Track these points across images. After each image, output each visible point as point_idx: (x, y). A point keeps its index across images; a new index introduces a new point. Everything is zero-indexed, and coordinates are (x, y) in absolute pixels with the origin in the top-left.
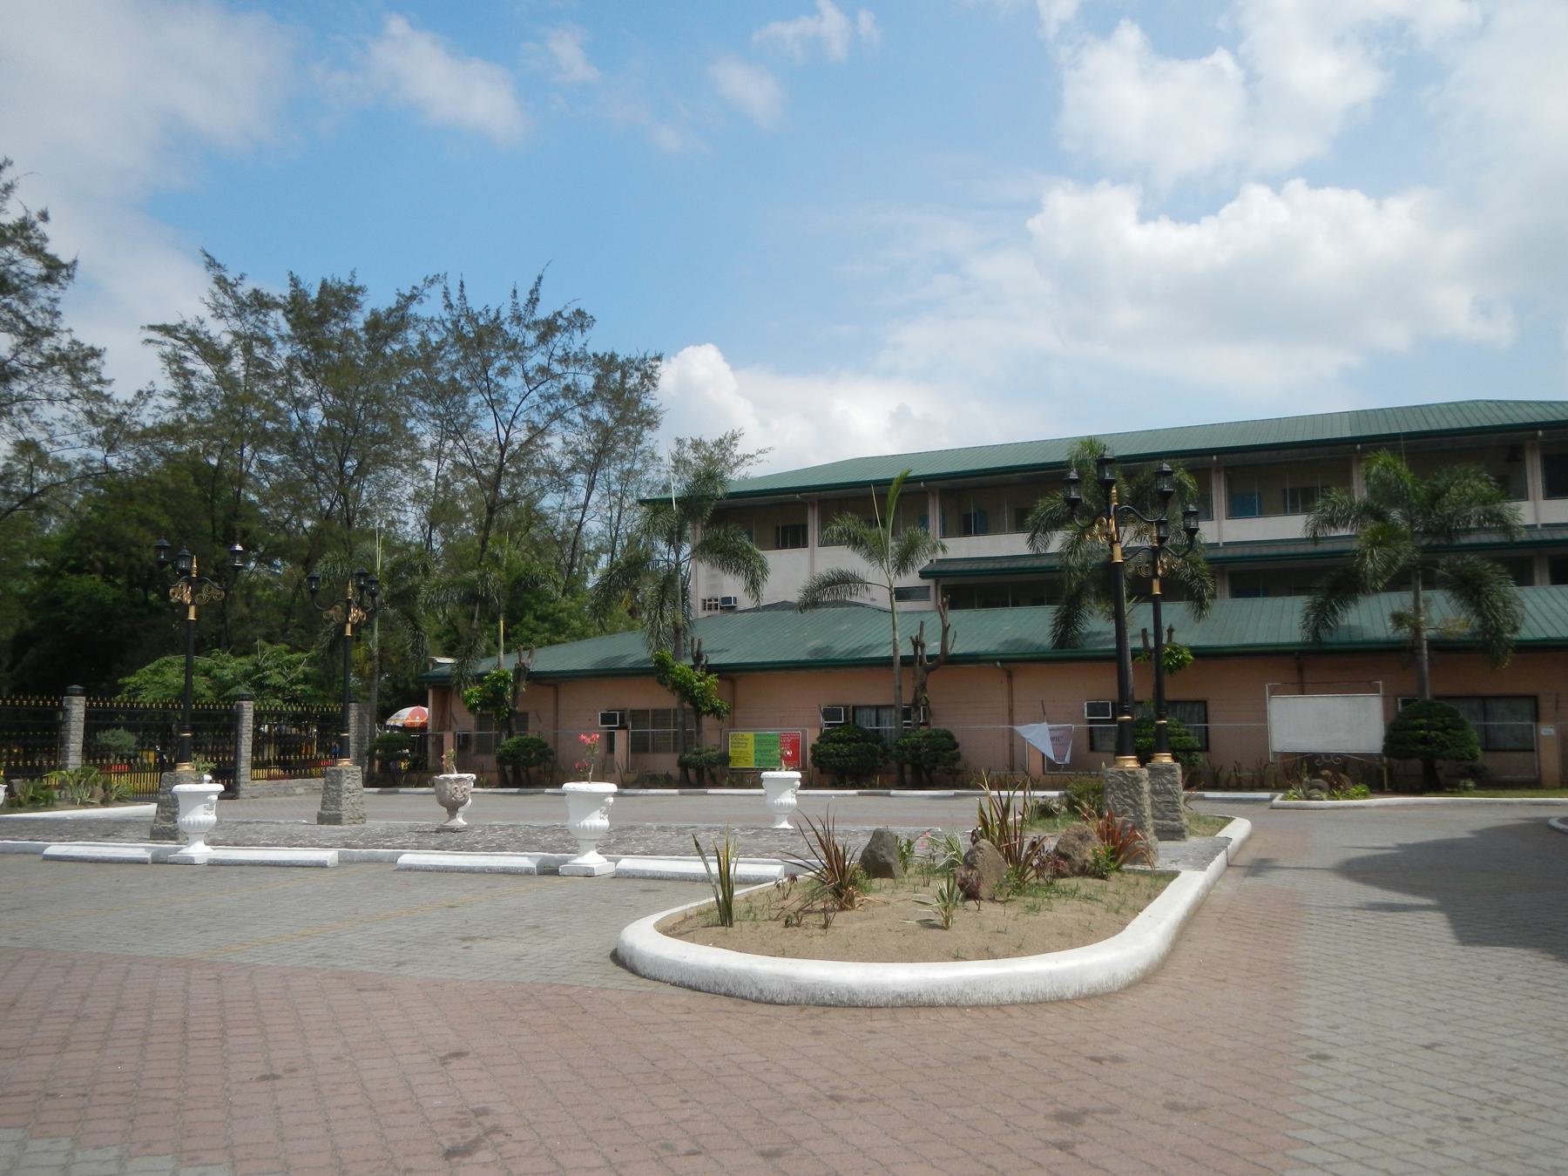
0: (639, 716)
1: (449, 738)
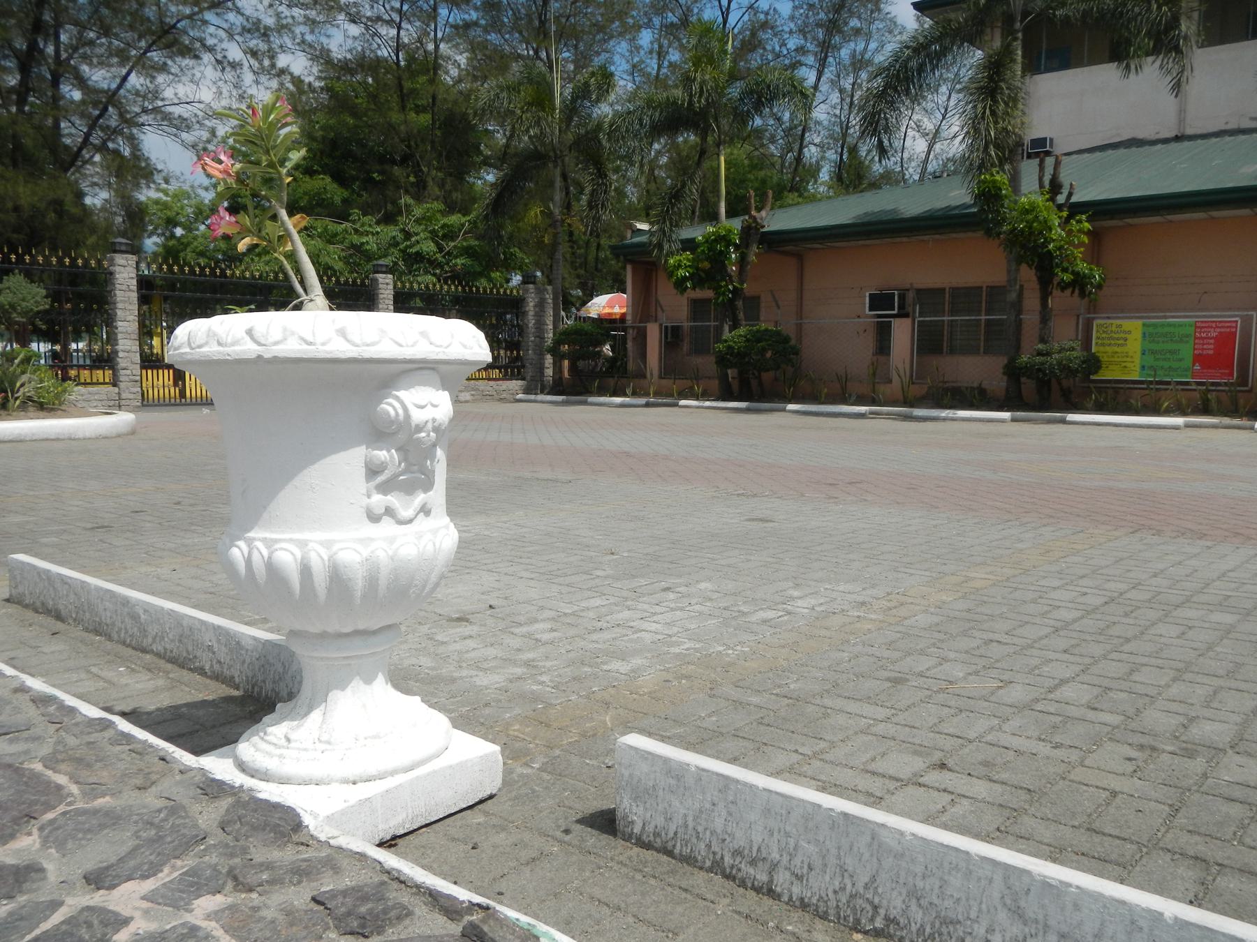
0: (931, 298)
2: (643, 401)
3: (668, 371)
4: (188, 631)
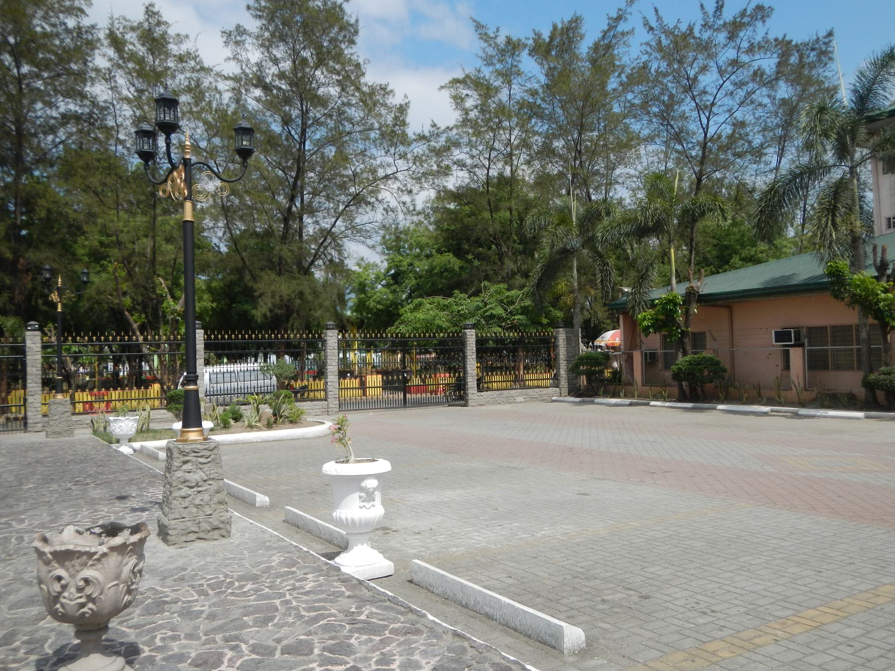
0: (816, 333)
2: (627, 401)
3: (647, 382)
4: (332, 533)
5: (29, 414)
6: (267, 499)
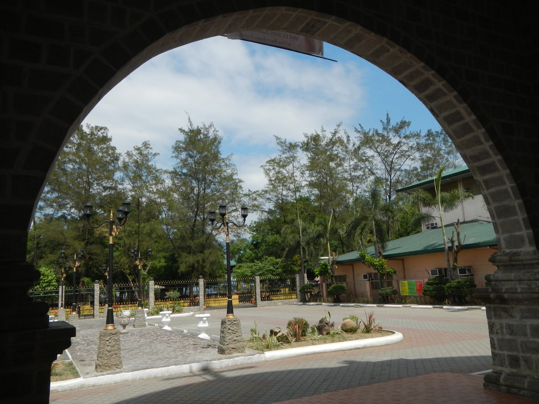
1: (324, 285)
5: (95, 312)
6: (157, 325)
